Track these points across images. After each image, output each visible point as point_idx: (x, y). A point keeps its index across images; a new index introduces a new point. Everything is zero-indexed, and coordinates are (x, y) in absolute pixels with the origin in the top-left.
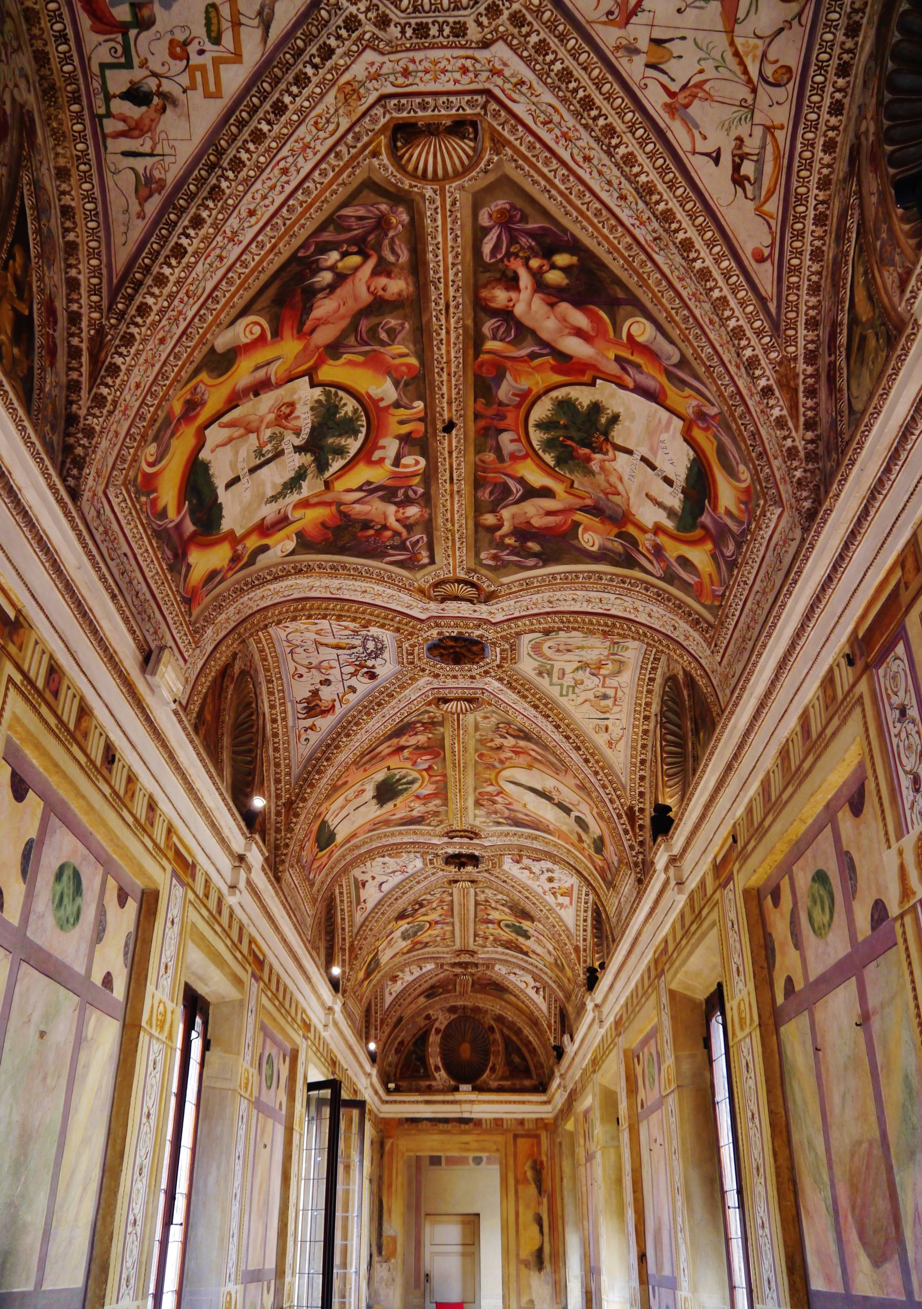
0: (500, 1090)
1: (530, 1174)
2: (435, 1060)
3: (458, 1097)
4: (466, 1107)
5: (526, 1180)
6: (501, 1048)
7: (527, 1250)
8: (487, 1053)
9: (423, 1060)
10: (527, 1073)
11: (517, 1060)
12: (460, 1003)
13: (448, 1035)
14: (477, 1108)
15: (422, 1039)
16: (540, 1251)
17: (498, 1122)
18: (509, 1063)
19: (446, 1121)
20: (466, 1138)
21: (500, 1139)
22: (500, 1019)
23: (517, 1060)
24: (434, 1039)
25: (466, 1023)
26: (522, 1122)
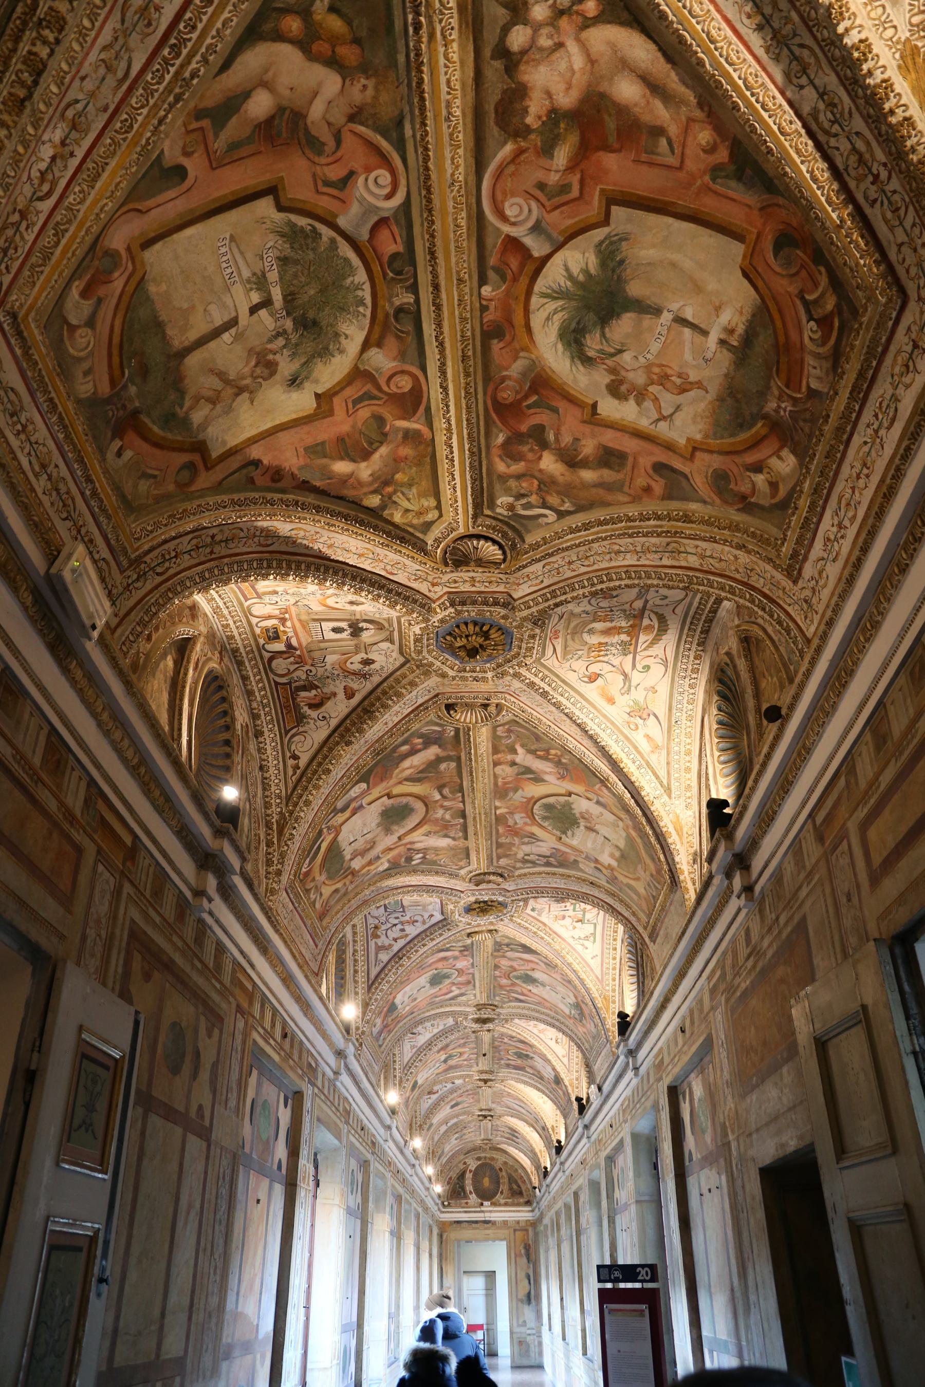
0: (506, 1204)
1: (523, 1251)
2: (469, 1187)
3: (483, 1209)
4: (487, 1214)
5: (521, 1255)
6: (506, 1180)
7: (522, 1293)
8: (498, 1183)
9: (463, 1188)
10: (521, 1194)
11: (515, 1187)
12: (483, 1155)
13: (476, 1173)
14: (493, 1215)
15: (462, 1176)
16: (529, 1293)
17: (505, 1223)
18: (511, 1189)
19: (476, 1222)
20: (488, 1232)
21: (506, 1232)
22: (505, 1163)
23: (515, 1187)
24: (469, 1176)
25: (486, 1168)
26: (518, 1222)
